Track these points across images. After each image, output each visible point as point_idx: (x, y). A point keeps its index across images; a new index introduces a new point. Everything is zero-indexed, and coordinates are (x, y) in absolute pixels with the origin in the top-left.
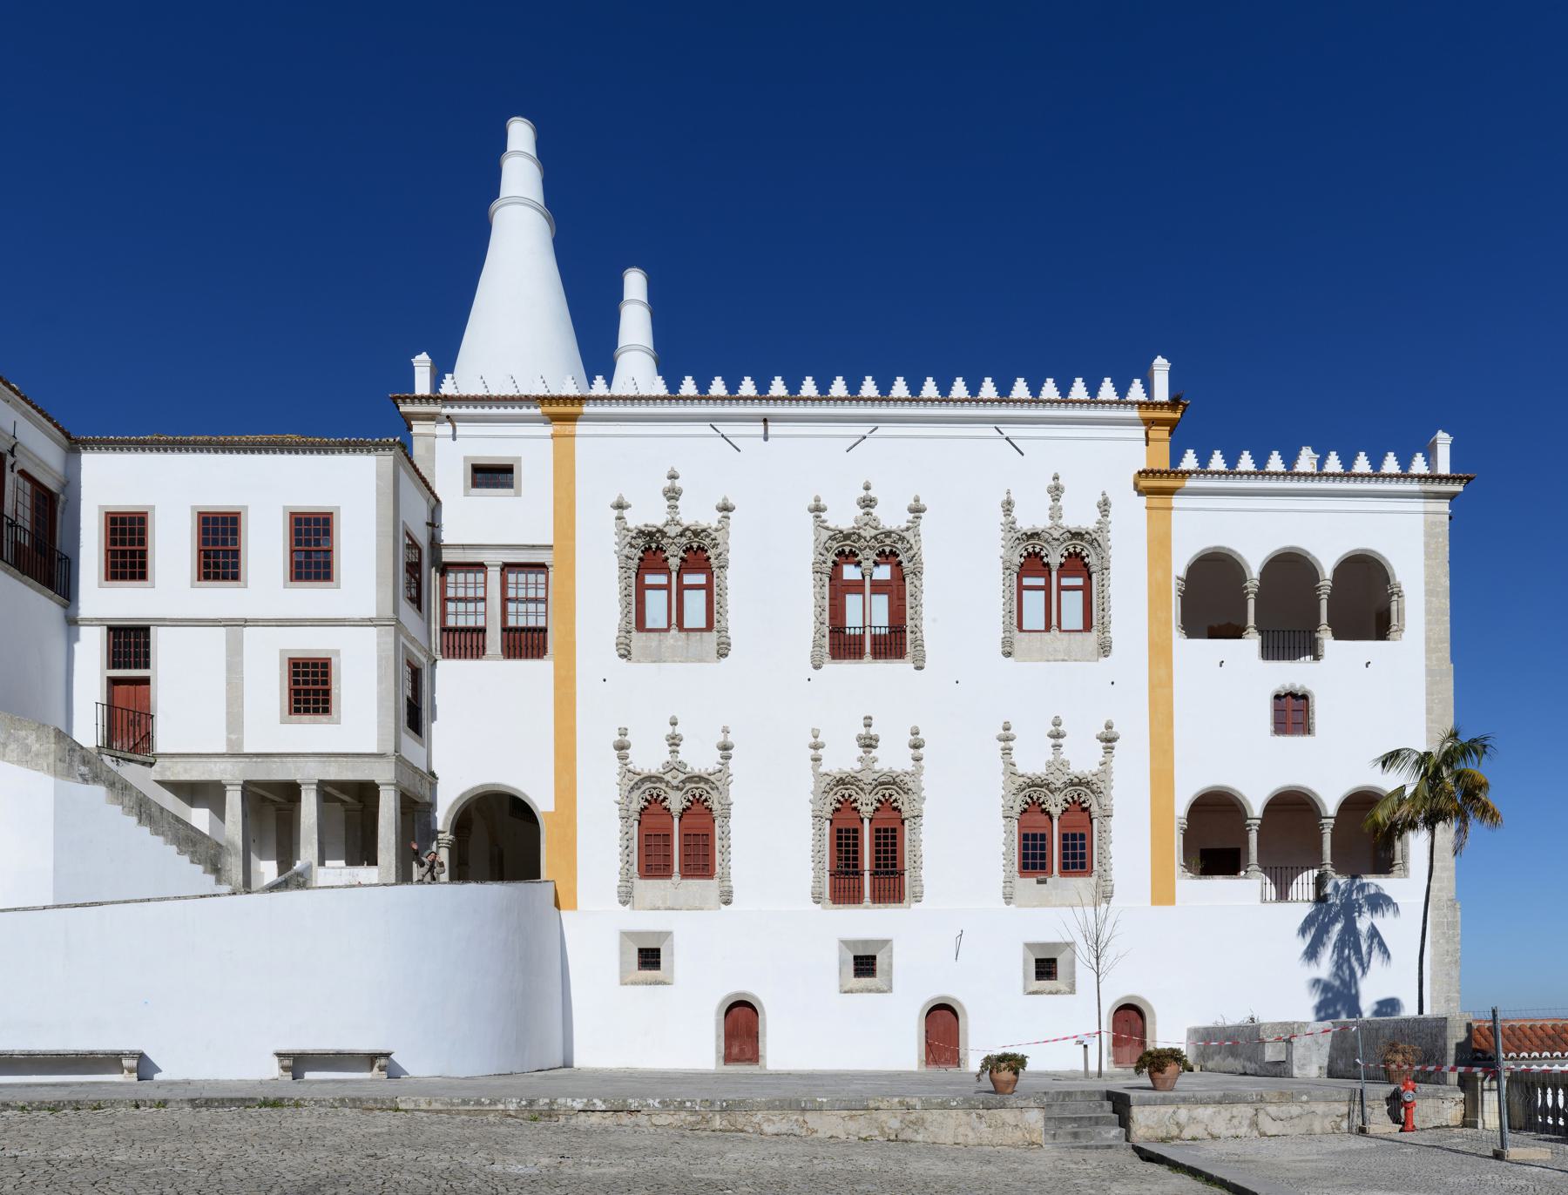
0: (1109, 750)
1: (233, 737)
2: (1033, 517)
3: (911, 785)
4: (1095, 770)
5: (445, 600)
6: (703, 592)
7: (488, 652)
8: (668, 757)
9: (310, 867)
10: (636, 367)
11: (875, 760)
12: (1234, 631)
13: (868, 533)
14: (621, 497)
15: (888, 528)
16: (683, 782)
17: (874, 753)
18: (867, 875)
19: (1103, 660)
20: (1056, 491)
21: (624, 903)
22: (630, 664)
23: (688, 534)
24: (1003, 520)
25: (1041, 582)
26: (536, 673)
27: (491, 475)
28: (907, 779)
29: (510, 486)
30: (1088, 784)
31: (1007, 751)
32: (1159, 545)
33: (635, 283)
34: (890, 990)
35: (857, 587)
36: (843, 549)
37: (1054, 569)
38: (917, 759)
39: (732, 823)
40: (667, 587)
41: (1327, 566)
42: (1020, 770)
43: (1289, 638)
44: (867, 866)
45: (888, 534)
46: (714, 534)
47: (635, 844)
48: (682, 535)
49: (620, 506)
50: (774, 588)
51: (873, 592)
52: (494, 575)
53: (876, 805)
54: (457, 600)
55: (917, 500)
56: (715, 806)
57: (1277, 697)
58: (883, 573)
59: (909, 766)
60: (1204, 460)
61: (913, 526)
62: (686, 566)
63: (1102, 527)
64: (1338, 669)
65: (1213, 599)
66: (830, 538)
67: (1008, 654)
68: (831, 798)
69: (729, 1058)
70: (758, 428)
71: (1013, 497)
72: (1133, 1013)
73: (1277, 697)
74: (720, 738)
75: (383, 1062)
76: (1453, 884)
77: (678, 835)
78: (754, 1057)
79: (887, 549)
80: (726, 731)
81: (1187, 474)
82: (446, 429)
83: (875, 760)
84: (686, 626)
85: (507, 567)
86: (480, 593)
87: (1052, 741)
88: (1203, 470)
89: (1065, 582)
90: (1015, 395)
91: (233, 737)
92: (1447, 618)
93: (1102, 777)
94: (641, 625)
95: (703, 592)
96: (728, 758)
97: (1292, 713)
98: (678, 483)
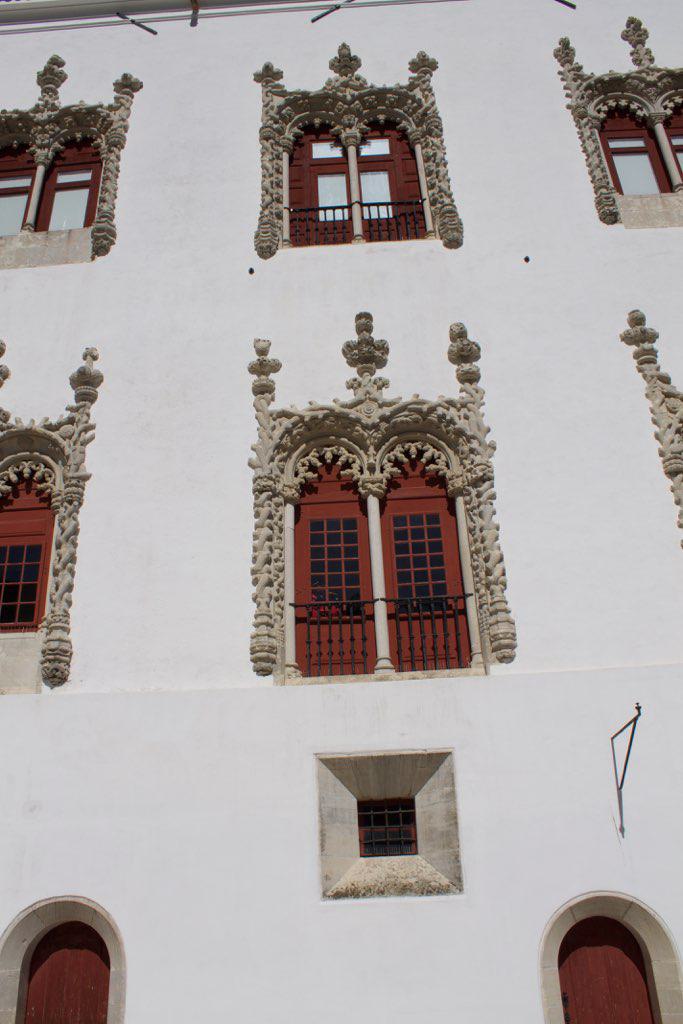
3: (461, 424)
11: (383, 384)
13: (349, 93)
15: (379, 85)
17: (379, 373)
18: (381, 611)
34: (456, 883)
38: (469, 378)
44: (379, 589)
45: (381, 93)
56: (58, 486)
59: (454, 390)
67: (610, 217)
83: (383, 384)
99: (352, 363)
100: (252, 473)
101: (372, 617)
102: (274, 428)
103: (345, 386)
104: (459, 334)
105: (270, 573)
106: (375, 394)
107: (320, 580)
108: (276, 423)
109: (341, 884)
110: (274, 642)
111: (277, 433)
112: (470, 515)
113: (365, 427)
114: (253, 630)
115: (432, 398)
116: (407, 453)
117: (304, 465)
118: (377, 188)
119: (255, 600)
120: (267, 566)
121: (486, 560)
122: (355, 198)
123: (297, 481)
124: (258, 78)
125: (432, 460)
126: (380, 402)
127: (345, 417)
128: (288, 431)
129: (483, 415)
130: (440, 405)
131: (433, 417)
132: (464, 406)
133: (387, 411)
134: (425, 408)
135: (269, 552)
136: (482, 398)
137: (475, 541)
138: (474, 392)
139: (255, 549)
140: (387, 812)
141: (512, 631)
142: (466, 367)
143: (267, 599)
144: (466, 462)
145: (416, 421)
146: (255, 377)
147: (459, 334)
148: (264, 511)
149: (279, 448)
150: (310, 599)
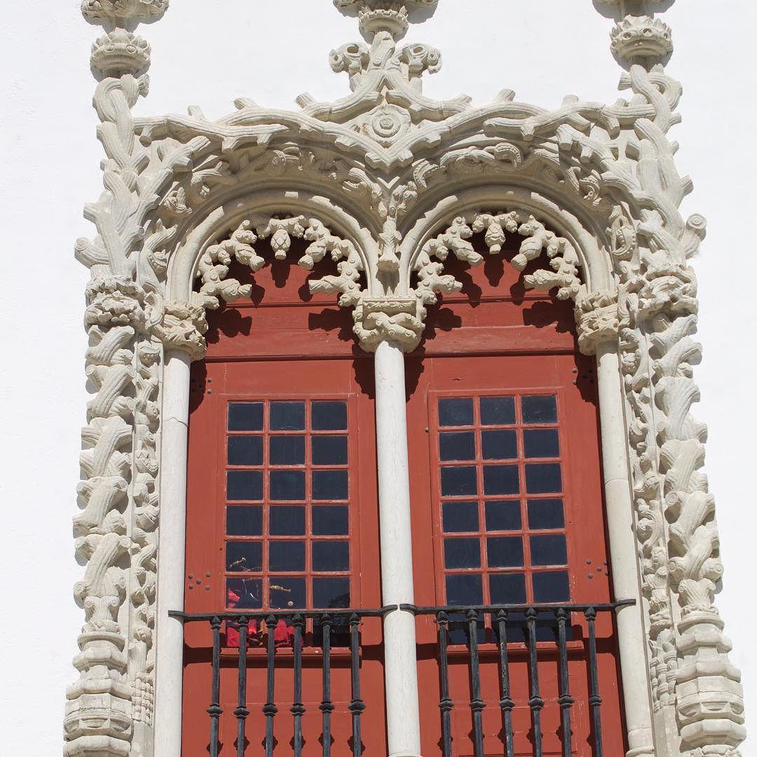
3: (618, 169)
11: (426, 64)
17: (416, 34)
18: (400, 636)
28: (596, 142)
38: (645, 54)
44: (398, 583)
59: (604, 85)
83: (426, 64)
100: (84, 278)
101: (377, 653)
102: (143, 165)
103: (327, 64)
105: (121, 531)
106: (403, 85)
107: (251, 555)
108: (151, 152)
110: (126, 710)
112: (632, 401)
113: (375, 171)
114: (75, 679)
116: (478, 240)
117: (216, 261)
119: (80, 599)
120: (115, 512)
121: (671, 515)
123: (200, 300)
125: (542, 260)
126: (415, 107)
127: (327, 142)
128: (179, 175)
129: (676, 149)
130: (566, 121)
131: (549, 151)
132: (627, 124)
133: (431, 132)
134: (528, 126)
135: (119, 478)
136: (673, 107)
137: (645, 466)
138: (653, 90)
139: (86, 471)
141: (735, 699)
142: (637, 24)
143: (114, 600)
144: (629, 267)
145: (506, 160)
146: (98, 32)
148: (113, 375)
149: (154, 214)
150: (220, 602)
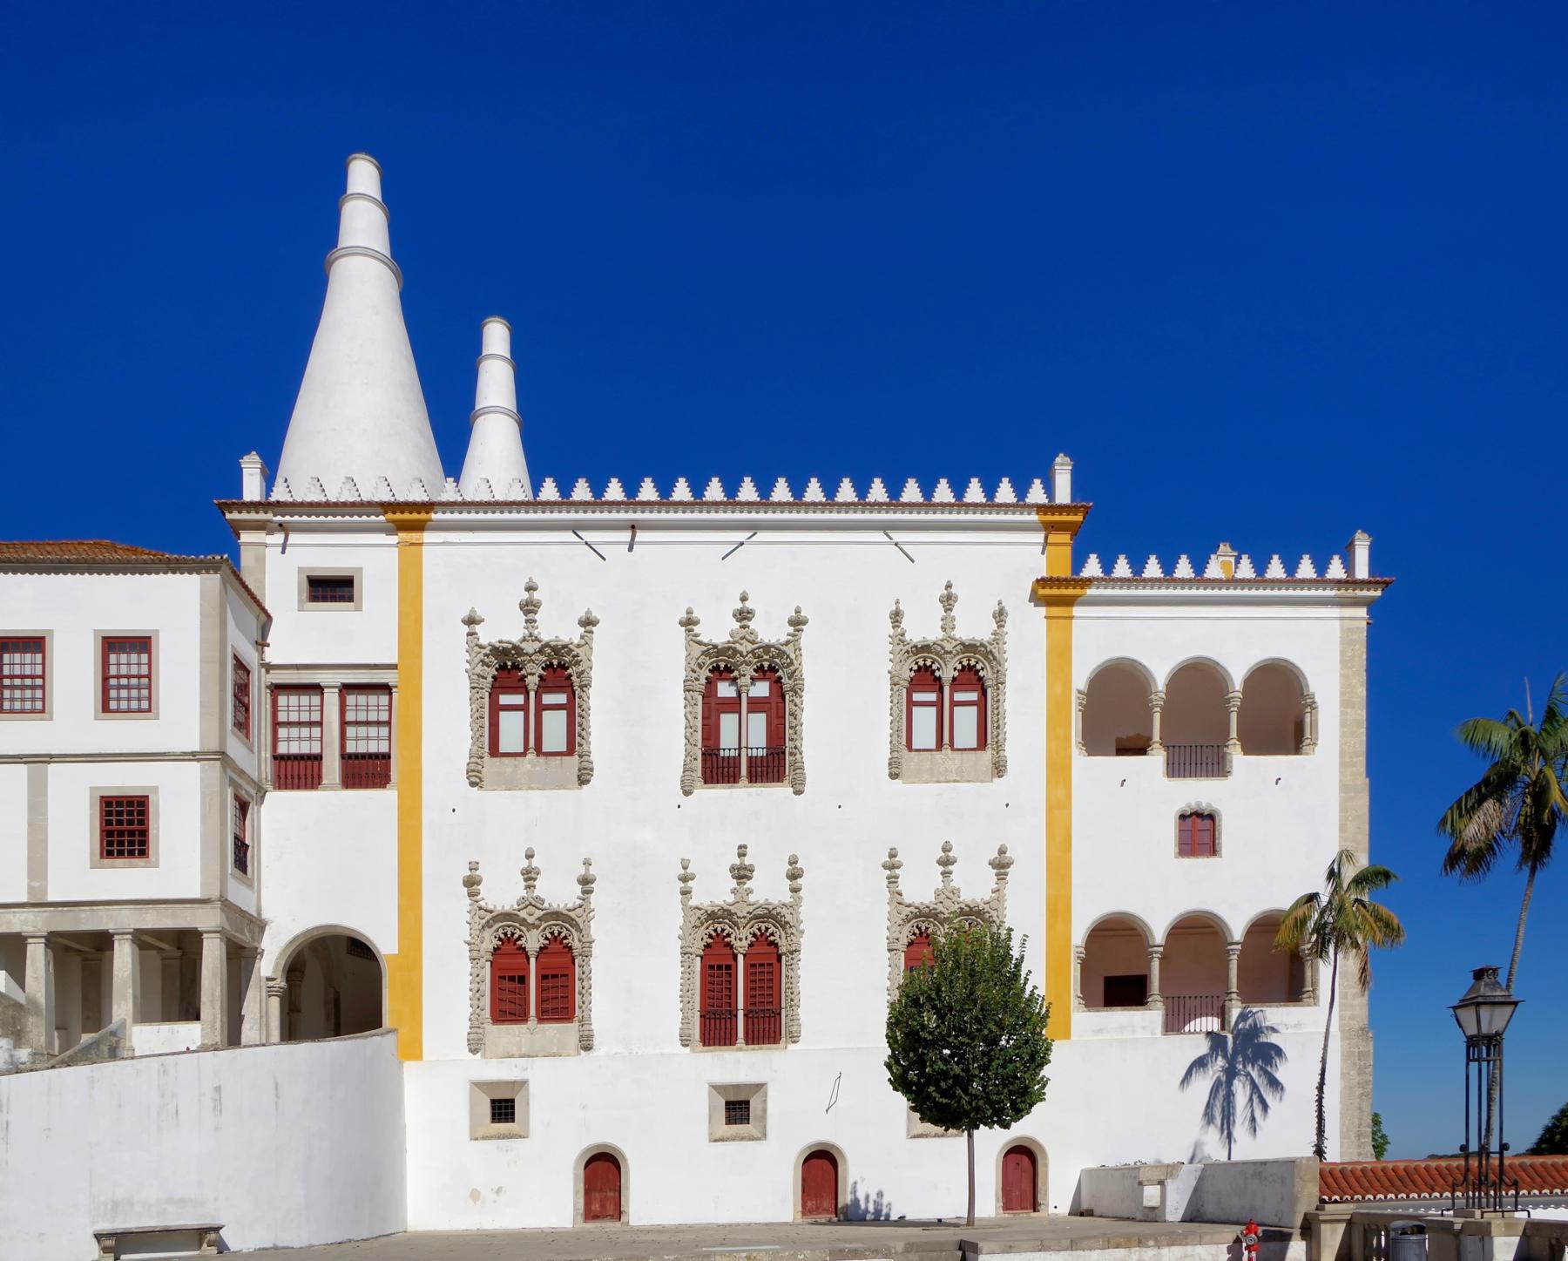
0: (1001, 877)
1: (36, 884)
2: (923, 627)
3: (788, 918)
4: (987, 898)
5: (276, 725)
6: (564, 713)
7: (324, 782)
8: (524, 893)
9: (123, 1024)
10: (497, 450)
11: (750, 891)
12: (1135, 747)
13: (745, 647)
14: (473, 610)
15: (766, 641)
16: (539, 919)
17: (749, 884)
18: (741, 1014)
19: (996, 780)
20: (948, 600)
21: (474, 1051)
22: (481, 792)
23: (548, 650)
24: (891, 632)
25: (932, 697)
26: (379, 803)
27: (330, 588)
28: (784, 911)
29: (350, 599)
30: (979, 913)
31: (893, 880)
32: (1059, 656)
33: (496, 336)
34: (764, 1135)
35: (732, 705)
36: (719, 665)
37: (947, 683)
38: (795, 890)
39: (593, 962)
40: (524, 708)
41: (1238, 675)
42: (907, 899)
43: (1197, 755)
44: (741, 1005)
45: (767, 648)
46: (577, 651)
47: (487, 987)
48: (541, 651)
49: (471, 621)
50: (640, 708)
51: (749, 712)
52: (332, 698)
53: (751, 939)
54: (289, 724)
55: (798, 611)
56: (576, 944)
57: (1183, 817)
58: (762, 689)
59: (787, 898)
60: (1108, 566)
61: (794, 639)
62: (545, 686)
63: (998, 637)
64: (1248, 787)
65: (1117, 715)
66: (703, 653)
67: (894, 776)
68: (702, 932)
69: (590, 1215)
70: (626, 536)
71: (901, 607)
72: (1025, 1160)
73: (1183, 817)
74: (582, 871)
75: (212, 1236)
76: (1365, 1012)
77: (535, 976)
78: (618, 1214)
79: (766, 664)
80: (587, 863)
81: (1088, 582)
82: (279, 538)
83: (750, 891)
84: (545, 749)
85: (346, 688)
86: (316, 717)
87: (941, 868)
88: (1108, 578)
89: (959, 697)
90: (905, 498)
91: (36, 884)
92: (1363, 731)
93: (994, 904)
94: (494, 750)
95: (564, 713)
96: (590, 892)
97: (1199, 833)
98: (536, 595)
99: (734, 877)
104: (793, 861)
109: (717, 1136)
111: (693, 919)
115: (775, 901)
118: (757, 729)
122: (744, 744)
124: (682, 624)
133: (751, 909)
140: (738, 1108)
147: (793, 861)
